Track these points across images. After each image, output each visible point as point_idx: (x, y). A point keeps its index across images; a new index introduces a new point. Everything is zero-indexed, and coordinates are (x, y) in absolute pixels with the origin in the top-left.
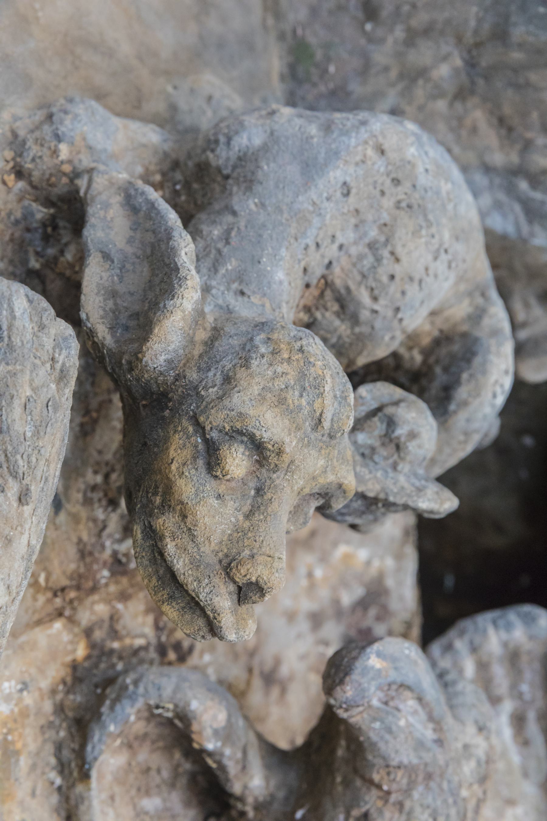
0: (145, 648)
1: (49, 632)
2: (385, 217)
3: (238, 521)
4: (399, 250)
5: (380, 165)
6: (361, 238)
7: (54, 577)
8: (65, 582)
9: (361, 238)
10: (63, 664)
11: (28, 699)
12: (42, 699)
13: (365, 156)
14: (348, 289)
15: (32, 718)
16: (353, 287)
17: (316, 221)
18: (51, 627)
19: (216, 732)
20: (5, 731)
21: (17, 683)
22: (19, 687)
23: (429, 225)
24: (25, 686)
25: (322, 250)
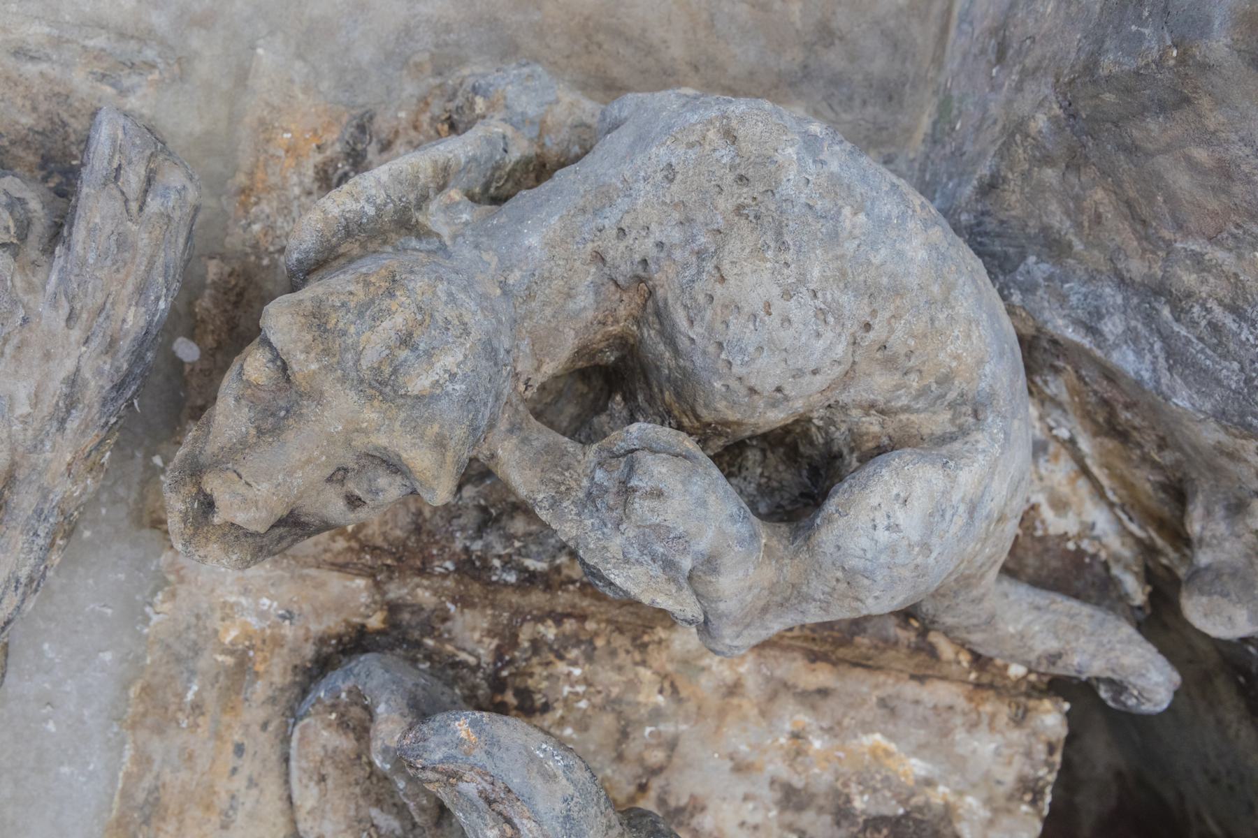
0: (475, 669)
1: (348, 583)
2: (720, 222)
3: (248, 433)
4: (726, 266)
5: (725, 154)
6: (687, 242)
7: (369, 531)
8: (379, 542)
9: (687, 242)
10: (348, 623)
11: (287, 630)
12: (306, 640)
13: (704, 138)
14: (666, 300)
15: (285, 650)
16: (670, 302)
17: (622, 203)
18: (352, 580)
19: (386, 751)
20: (247, 643)
21: (280, 607)
22: (281, 612)
23: (782, 246)
24: (289, 616)
25: (629, 240)
